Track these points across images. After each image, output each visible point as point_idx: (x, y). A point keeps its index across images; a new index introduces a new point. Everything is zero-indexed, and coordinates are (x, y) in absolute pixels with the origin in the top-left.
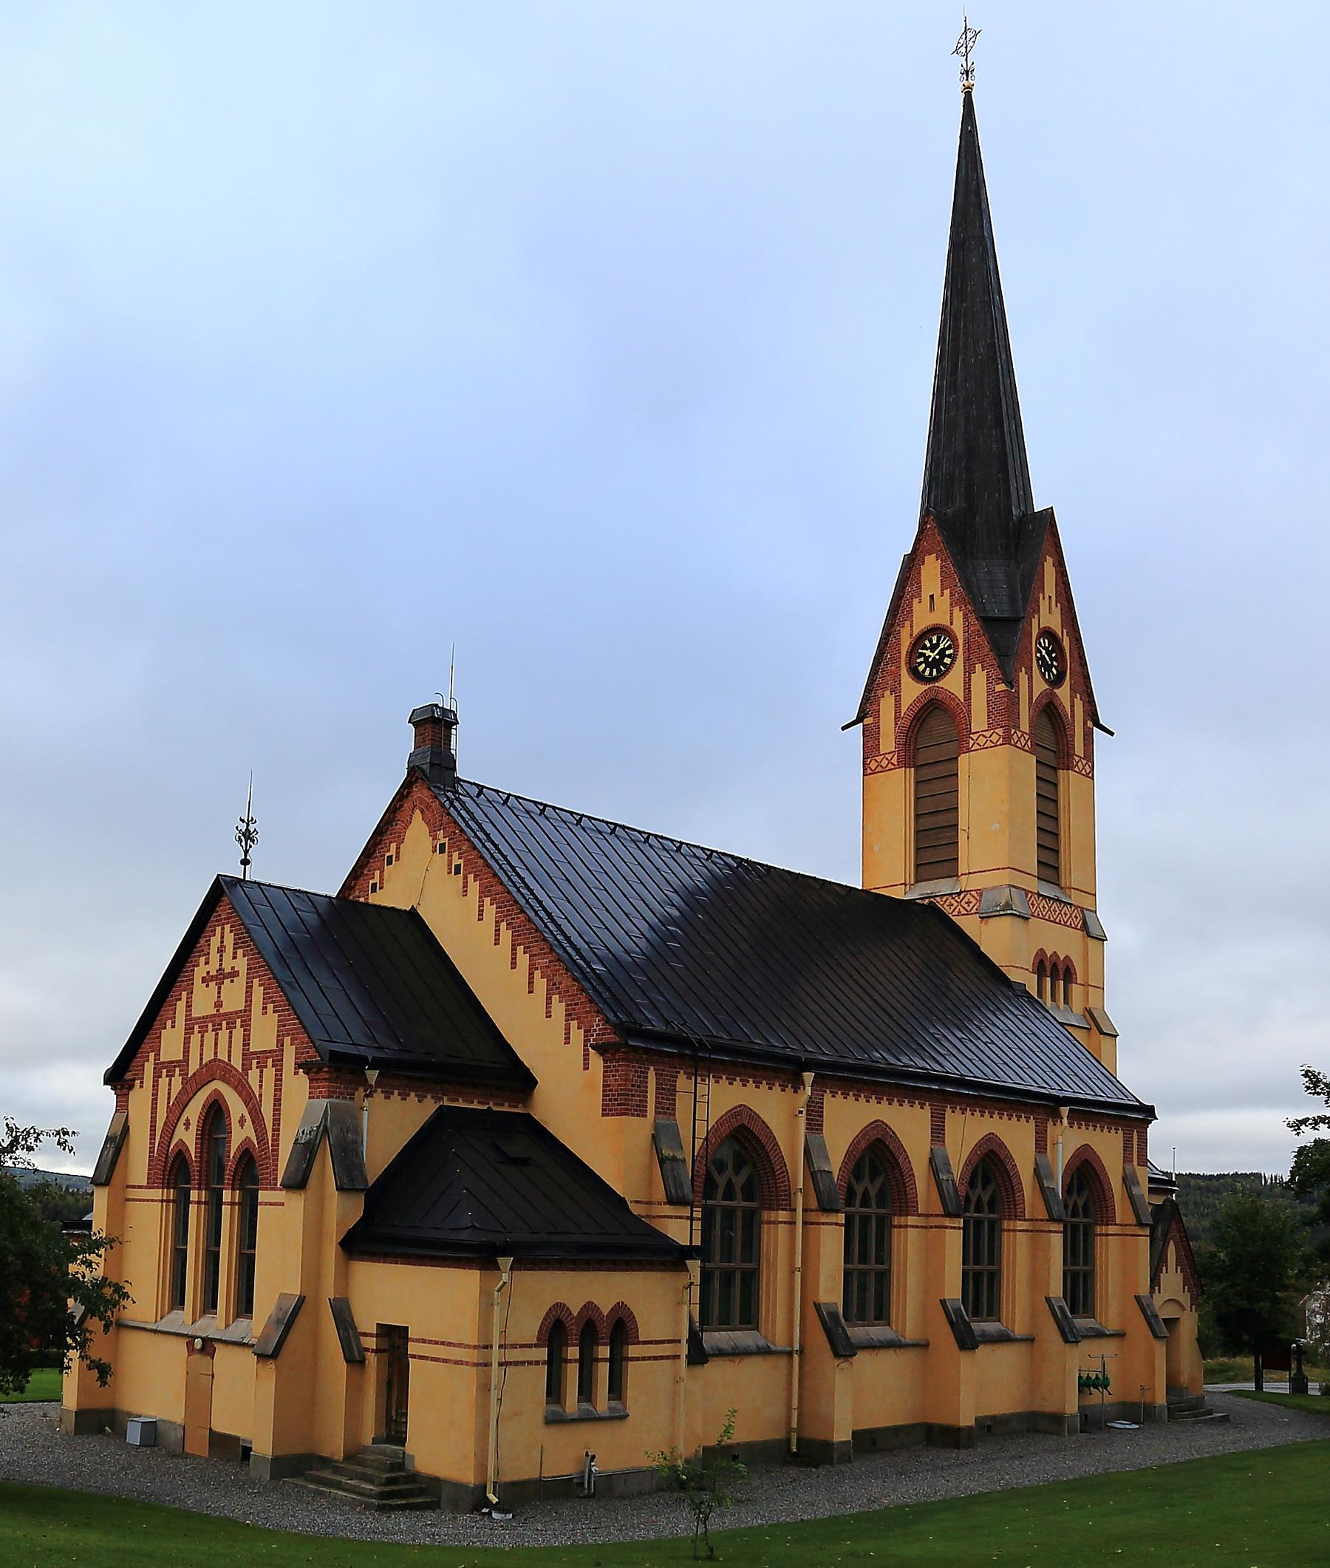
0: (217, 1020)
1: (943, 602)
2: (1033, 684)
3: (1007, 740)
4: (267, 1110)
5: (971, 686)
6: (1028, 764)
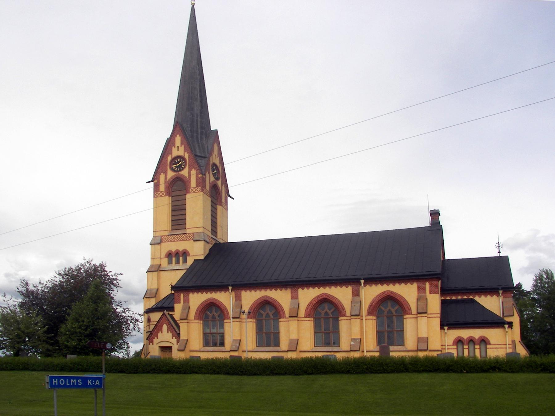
1: (182, 149)
2: (210, 178)
5: (190, 174)
6: (209, 200)
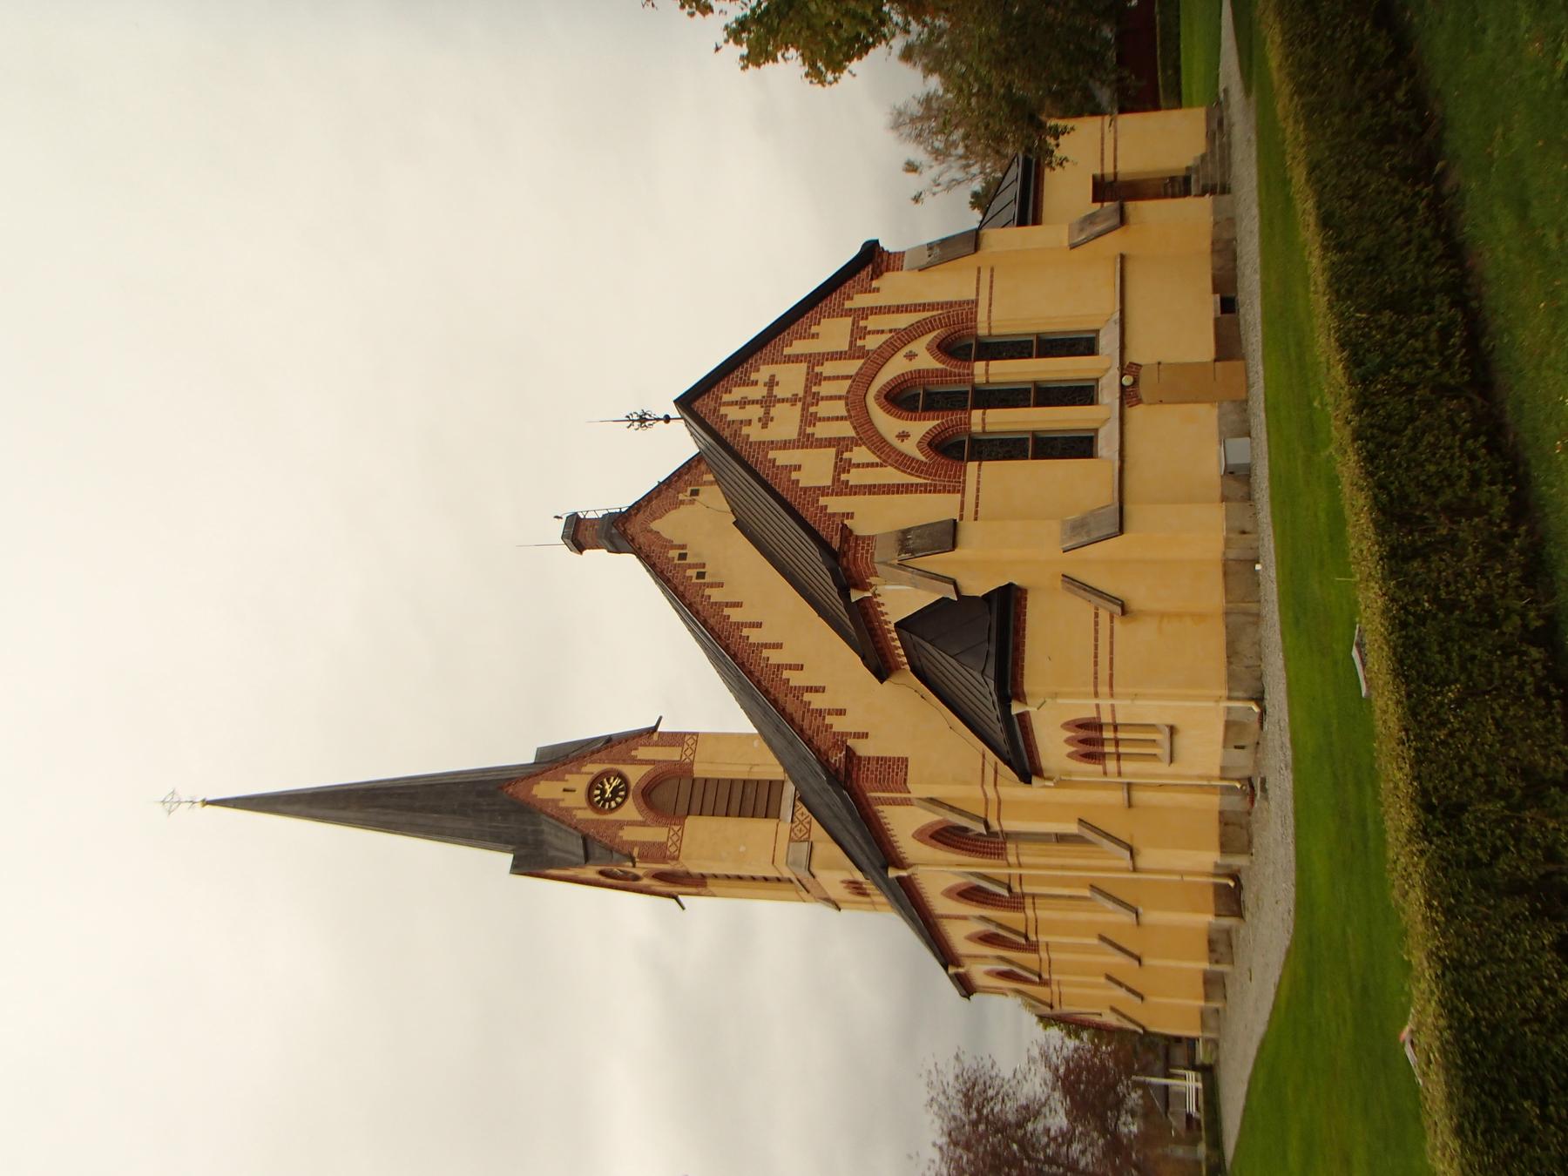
0: (809, 399)
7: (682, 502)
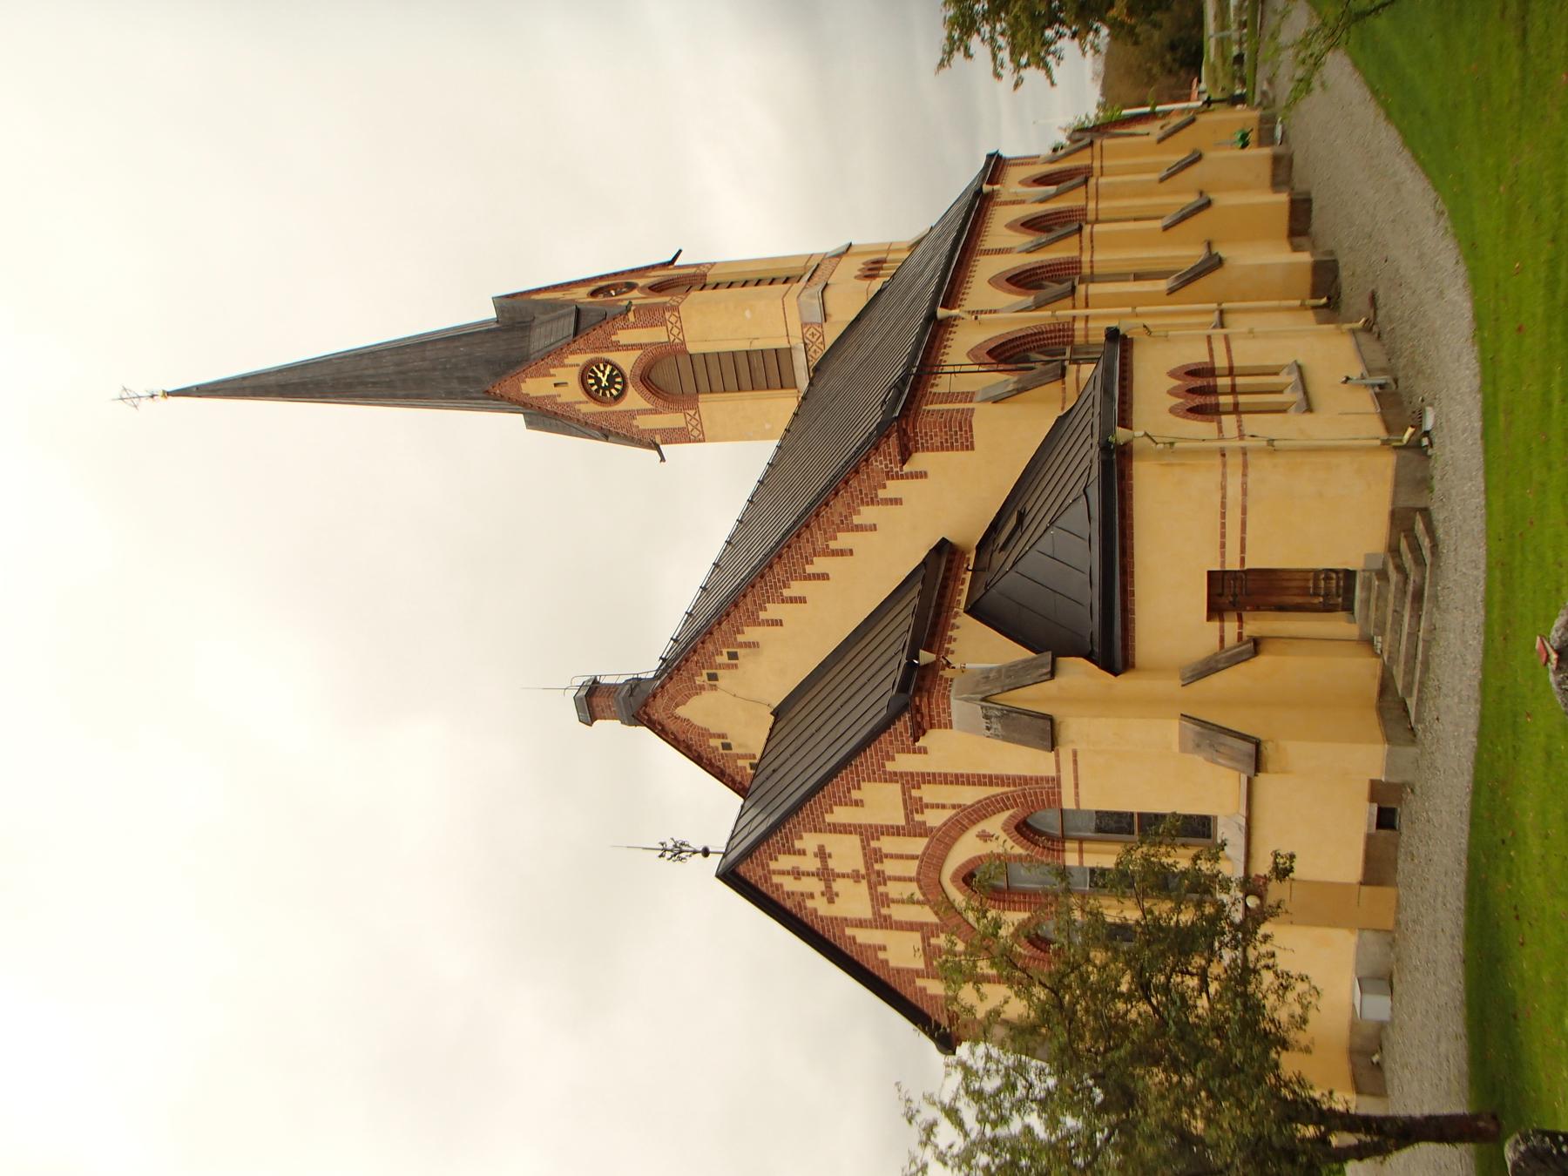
0: (874, 878)
3: (675, 309)
4: (970, 795)
7: (702, 688)
